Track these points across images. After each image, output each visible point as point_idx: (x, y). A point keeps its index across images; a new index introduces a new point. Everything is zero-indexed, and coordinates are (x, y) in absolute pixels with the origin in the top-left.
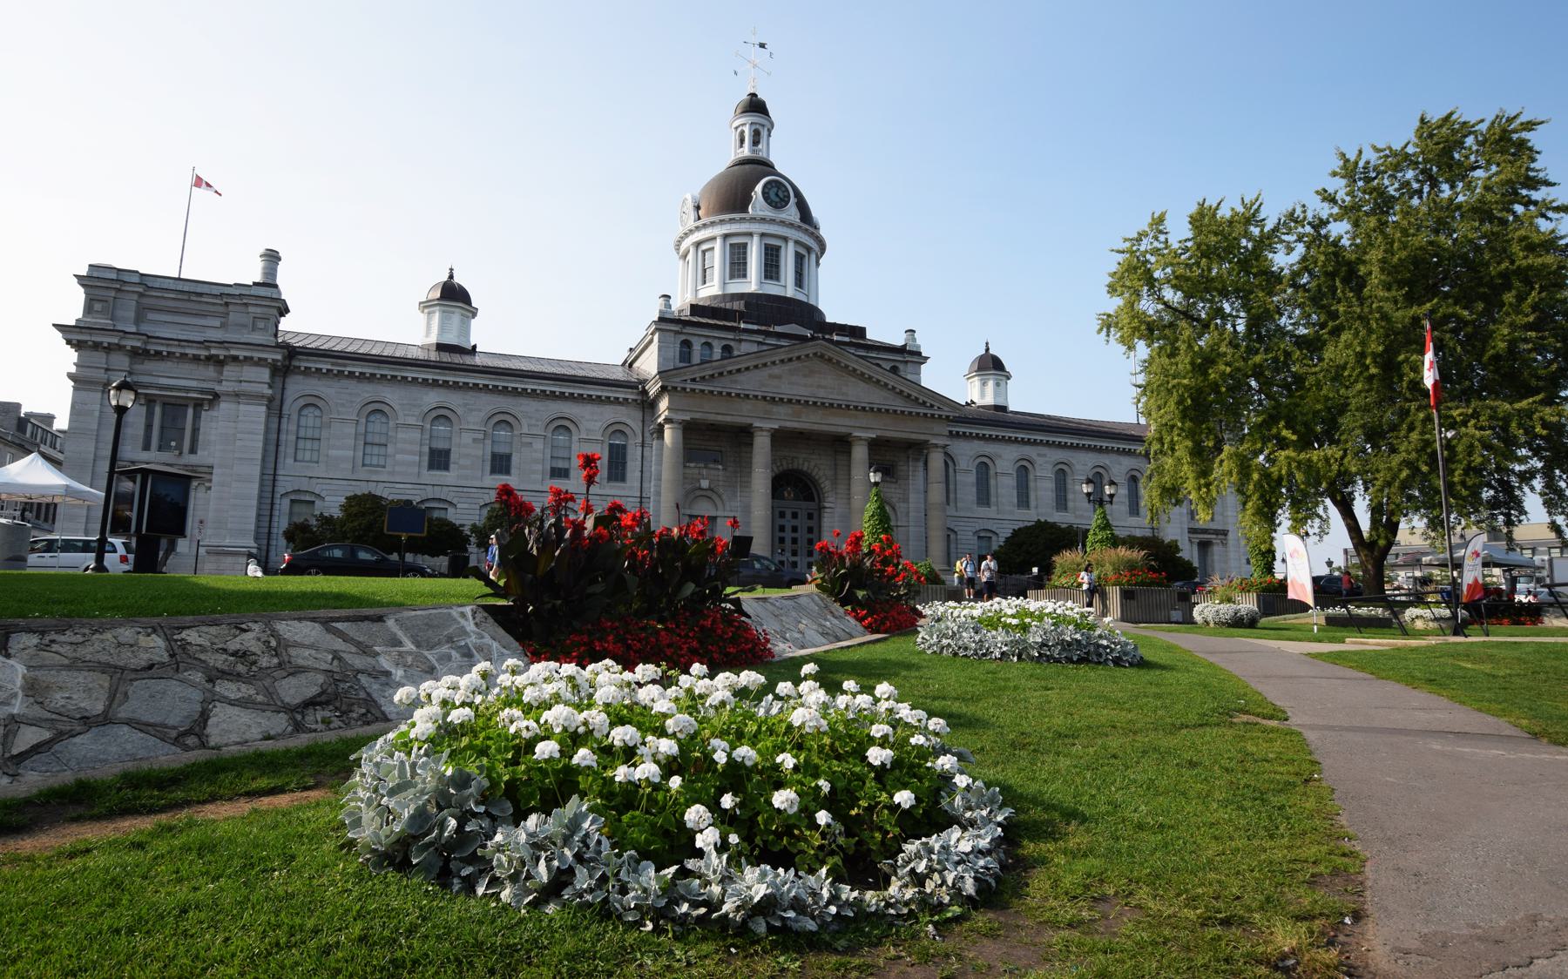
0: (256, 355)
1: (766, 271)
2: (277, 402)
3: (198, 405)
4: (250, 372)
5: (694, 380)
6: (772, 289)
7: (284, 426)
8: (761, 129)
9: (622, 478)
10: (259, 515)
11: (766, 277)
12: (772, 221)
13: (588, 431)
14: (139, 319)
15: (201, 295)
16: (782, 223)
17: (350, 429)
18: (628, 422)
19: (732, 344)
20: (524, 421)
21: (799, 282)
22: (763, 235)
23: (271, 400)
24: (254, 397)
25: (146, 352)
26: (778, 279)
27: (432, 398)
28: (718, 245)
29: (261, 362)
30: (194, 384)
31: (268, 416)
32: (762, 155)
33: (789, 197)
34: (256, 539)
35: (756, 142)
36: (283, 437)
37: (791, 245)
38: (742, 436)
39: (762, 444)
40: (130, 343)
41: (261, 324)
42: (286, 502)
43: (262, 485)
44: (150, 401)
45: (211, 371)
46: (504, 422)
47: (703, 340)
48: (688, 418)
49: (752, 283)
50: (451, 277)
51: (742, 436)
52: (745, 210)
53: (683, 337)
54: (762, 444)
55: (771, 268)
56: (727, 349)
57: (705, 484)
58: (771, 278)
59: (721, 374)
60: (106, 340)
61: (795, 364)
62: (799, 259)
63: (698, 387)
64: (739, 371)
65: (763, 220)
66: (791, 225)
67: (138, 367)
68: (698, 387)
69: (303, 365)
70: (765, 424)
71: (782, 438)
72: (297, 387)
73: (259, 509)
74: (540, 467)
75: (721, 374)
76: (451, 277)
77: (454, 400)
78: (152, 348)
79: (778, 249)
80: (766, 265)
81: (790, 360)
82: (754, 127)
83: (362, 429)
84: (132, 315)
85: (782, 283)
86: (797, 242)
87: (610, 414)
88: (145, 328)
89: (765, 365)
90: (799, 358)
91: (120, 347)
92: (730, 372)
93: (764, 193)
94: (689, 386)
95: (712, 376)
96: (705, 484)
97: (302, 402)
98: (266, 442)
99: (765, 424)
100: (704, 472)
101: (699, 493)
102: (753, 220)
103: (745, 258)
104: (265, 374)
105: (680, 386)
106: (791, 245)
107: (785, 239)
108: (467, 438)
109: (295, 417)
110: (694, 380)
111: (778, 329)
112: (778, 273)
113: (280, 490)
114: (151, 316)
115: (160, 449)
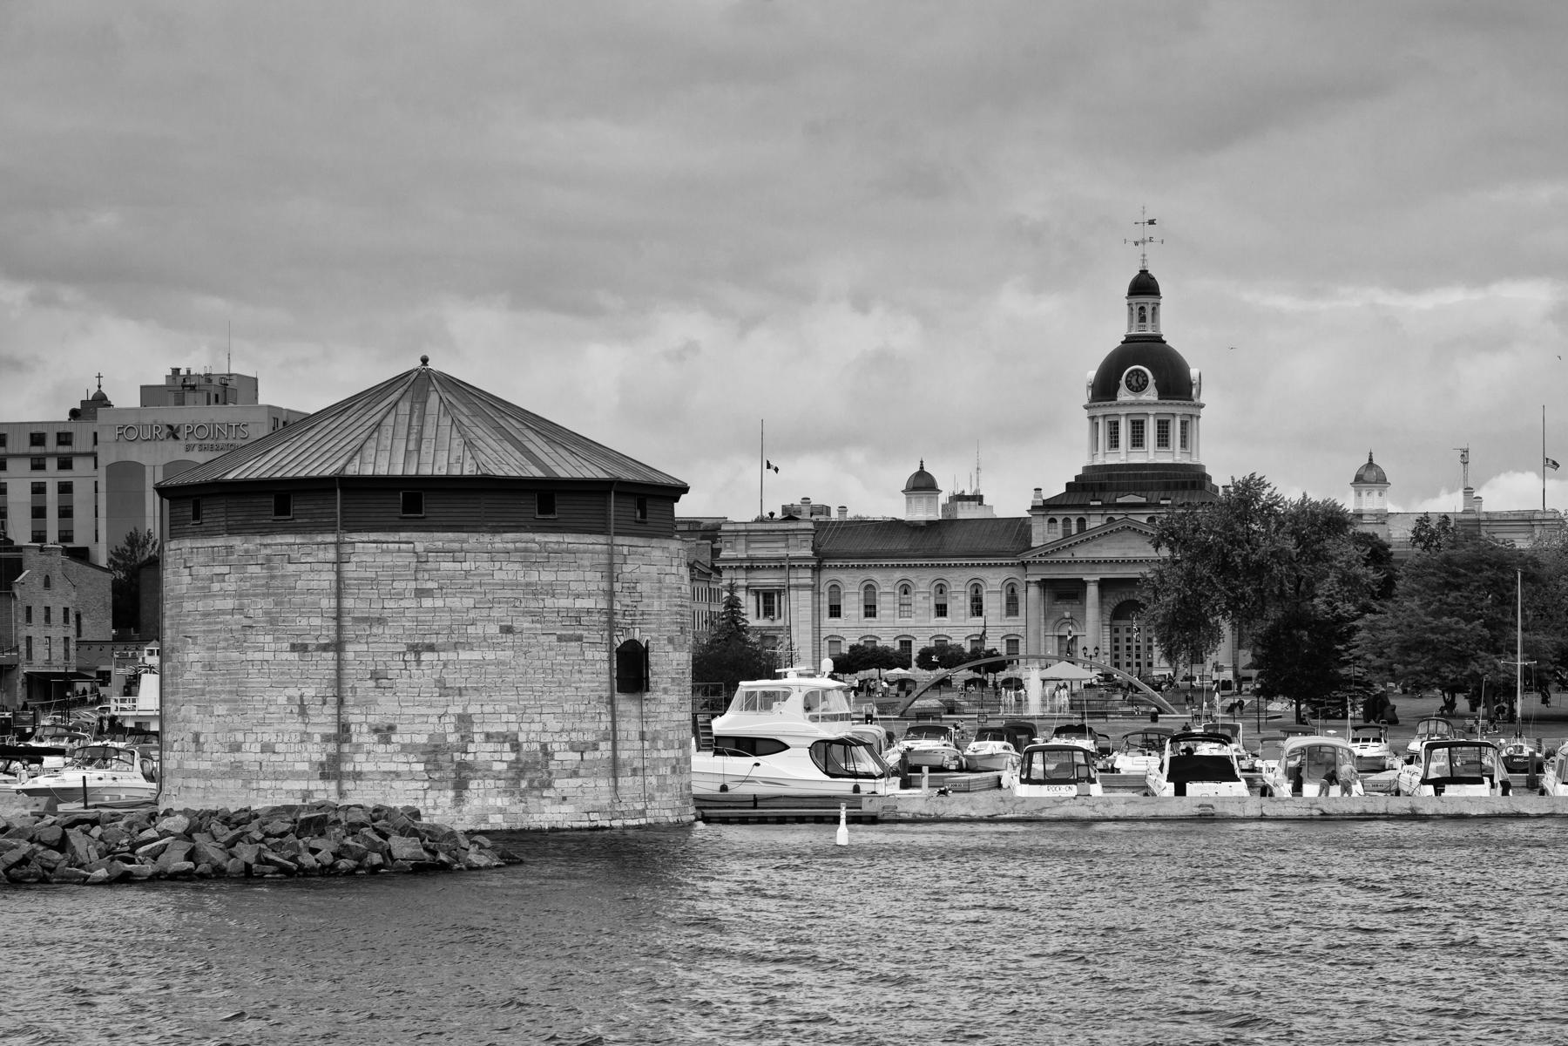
0: (803, 564)
2: (817, 586)
3: (779, 593)
4: (801, 573)
5: (1040, 555)
6: (1138, 458)
7: (821, 599)
8: (1145, 306)
9: (1016, 613)
10: (813, 651)
11: (1134, 445)
12: (1132, 404)
13: (992, 585)
14: (747, 548)
15: (773, 531)
16: (1140, 404)
17: (855, 598)
18: (1014, 576)
19: (1084, 517)
20: (952, 584)
21: (1163, 440)
22: (1127, 415)
23: (813, 586)
24: (805, 586)
25: (752, 567)
27: (898, 575)
29: (807, 567)
30: (776, 581)
31: (813, 598)
33: (1147, 381)
34: (813, 664)
36: (821, 606)
37: (1151, 418)
38: (1081, 585)
39: (1092, 592)
40: (745, 565)
41: (804, 544)
42: (827, 642)
43: (813, 634)
44: (757, 593)
45: (783, 574)
46: (941, 589)
47: (1063, 517)
48: (1039, 579)
49: (1125, 455)
50: (922, 468)
51: (1081, 585)
52: (1114, 398)
53: (1049, 517)
54: (1092, 592)
56: (1081, 522)
57: (1067, 615)
59: (1058, 549)
60: (734, 565)
61: (1112, 535)
62: (1163, 428)
63: (1043, 559)
64: (1070, 545)
65: (1124, 404)
66: (1148, 404)
67: (750, 575)
68: (1043, 559)
69: (828, 564)
70: (1092, 577)
71: (1104, 585)
72: (827, 577)
73: (813, 647)
74: (963, 611)
75: (1058, 549)
76: (922, 468)
77: (911, 575)
78: (755, 565)
79: (1142, 422)
81: (1106, 533)
83: (862, 596)
84: (744, 547)
87: (1004, 574)
88: (750, 553)
89: (1088, 539)
90: (1111, 531)
91: (741, 567)
92: (1064, 547)
93: (1126, 382)
94: (1037, 560)
95: (1052, 551)
96: (1067, 615)
97: (830, 584)
98: (813, 610)
99: (1092, 577)
100: (1067, 607)
101: (1064, 621)
102: (1118, 405)
104: (809, 573)
105: (1032, 560)
106: (1151, 418)
108: (919, 597)
109: (827, 593)
110: (1040, 555)
111: (1119, 500)
113: (823, 636)
114: (753, 545)
115: (766, 615)
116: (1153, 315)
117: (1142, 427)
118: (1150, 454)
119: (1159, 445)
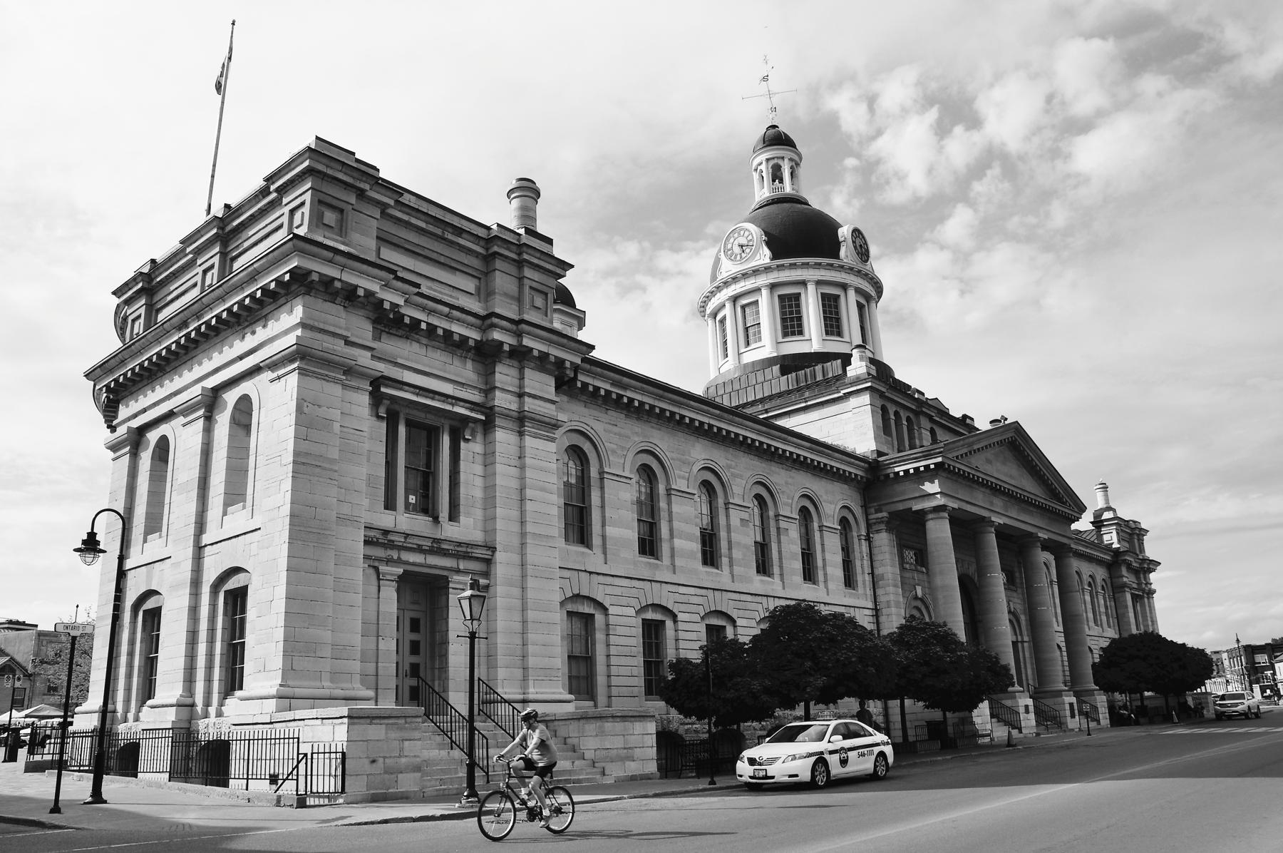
1: (784, 327)
6: (795, 347)
8: (780, 162)
11: (785, 335)
21: (833, 325)
22: (773, 287)
26: (801, 333)
28: (727, 311)
32: (788, 188)
35: (777, 175)
37: (811, 287)
55: (791, 323)
58: (793, 334)
79: (797, 297)
80: (783, 320)
82: (771, 163)
85: (807, 337)
86: (819, 283)
103: (799, 312)
106: (811, 287)
107: (803, 283)
112: (800, 326)
116: (792, 174)
117: (798, 306)
118: (813, 339)
119: (827, 333)
